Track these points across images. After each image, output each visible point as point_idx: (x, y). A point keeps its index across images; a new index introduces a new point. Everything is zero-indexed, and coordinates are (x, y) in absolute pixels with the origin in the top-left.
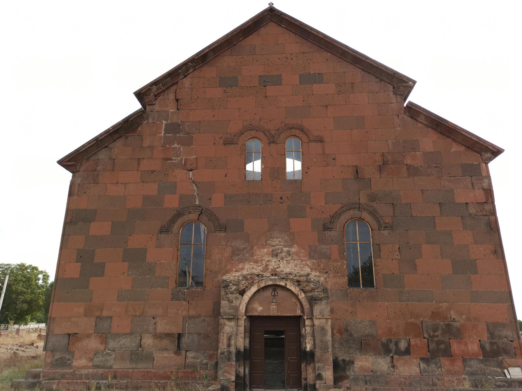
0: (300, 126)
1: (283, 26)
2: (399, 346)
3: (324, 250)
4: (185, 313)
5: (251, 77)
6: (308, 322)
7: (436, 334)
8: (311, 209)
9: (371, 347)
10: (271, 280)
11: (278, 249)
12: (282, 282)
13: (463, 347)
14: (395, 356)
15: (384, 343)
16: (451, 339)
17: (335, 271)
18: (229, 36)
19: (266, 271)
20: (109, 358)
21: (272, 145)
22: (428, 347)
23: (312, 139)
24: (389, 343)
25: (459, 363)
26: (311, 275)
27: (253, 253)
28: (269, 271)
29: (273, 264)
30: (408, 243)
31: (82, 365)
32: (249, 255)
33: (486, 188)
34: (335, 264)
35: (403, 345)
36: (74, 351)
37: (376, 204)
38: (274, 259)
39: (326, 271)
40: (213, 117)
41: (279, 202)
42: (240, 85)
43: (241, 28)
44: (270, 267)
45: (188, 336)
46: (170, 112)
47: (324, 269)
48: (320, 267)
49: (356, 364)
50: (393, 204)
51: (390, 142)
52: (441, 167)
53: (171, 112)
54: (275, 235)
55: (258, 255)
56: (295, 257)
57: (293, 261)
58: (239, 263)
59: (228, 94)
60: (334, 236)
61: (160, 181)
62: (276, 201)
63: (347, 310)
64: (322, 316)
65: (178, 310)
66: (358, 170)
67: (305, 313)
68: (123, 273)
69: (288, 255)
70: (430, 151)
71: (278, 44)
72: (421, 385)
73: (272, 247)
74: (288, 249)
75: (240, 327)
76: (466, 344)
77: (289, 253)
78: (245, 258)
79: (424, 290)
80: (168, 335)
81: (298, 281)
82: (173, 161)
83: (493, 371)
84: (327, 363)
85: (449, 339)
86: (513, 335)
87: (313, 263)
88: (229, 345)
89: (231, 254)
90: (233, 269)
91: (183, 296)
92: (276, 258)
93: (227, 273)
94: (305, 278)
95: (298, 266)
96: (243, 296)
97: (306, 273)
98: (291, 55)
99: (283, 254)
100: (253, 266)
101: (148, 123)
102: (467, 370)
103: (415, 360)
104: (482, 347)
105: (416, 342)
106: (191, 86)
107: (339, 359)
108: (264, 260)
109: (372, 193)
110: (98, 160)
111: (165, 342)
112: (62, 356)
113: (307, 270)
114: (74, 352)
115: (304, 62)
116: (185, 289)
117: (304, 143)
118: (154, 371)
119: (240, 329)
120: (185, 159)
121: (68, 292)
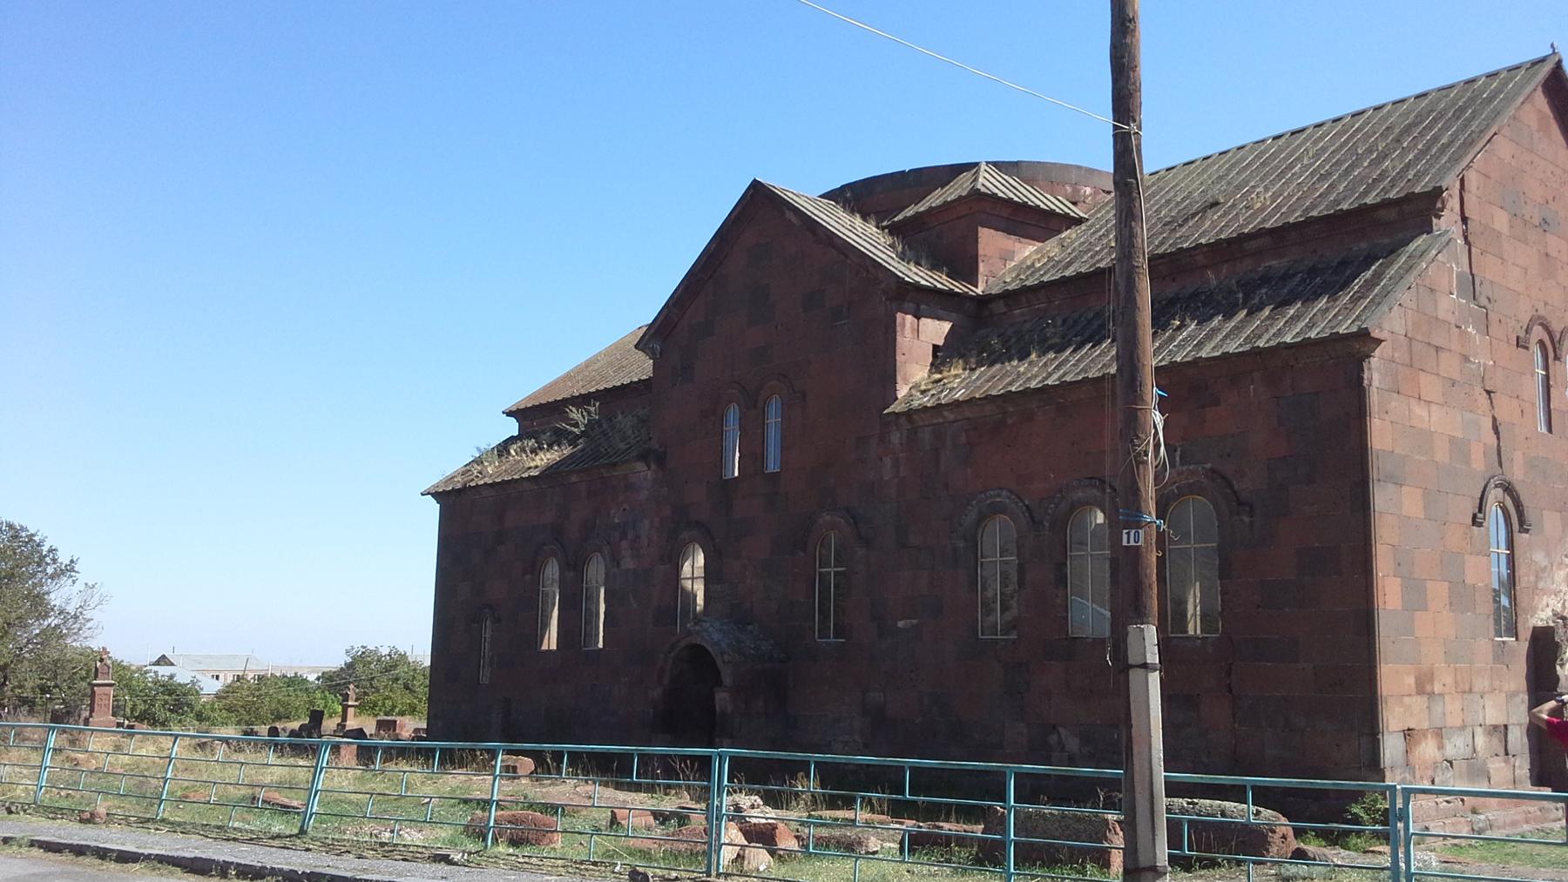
4: (1506, 688)
80: (1495, 727)
112: (1403, 776)
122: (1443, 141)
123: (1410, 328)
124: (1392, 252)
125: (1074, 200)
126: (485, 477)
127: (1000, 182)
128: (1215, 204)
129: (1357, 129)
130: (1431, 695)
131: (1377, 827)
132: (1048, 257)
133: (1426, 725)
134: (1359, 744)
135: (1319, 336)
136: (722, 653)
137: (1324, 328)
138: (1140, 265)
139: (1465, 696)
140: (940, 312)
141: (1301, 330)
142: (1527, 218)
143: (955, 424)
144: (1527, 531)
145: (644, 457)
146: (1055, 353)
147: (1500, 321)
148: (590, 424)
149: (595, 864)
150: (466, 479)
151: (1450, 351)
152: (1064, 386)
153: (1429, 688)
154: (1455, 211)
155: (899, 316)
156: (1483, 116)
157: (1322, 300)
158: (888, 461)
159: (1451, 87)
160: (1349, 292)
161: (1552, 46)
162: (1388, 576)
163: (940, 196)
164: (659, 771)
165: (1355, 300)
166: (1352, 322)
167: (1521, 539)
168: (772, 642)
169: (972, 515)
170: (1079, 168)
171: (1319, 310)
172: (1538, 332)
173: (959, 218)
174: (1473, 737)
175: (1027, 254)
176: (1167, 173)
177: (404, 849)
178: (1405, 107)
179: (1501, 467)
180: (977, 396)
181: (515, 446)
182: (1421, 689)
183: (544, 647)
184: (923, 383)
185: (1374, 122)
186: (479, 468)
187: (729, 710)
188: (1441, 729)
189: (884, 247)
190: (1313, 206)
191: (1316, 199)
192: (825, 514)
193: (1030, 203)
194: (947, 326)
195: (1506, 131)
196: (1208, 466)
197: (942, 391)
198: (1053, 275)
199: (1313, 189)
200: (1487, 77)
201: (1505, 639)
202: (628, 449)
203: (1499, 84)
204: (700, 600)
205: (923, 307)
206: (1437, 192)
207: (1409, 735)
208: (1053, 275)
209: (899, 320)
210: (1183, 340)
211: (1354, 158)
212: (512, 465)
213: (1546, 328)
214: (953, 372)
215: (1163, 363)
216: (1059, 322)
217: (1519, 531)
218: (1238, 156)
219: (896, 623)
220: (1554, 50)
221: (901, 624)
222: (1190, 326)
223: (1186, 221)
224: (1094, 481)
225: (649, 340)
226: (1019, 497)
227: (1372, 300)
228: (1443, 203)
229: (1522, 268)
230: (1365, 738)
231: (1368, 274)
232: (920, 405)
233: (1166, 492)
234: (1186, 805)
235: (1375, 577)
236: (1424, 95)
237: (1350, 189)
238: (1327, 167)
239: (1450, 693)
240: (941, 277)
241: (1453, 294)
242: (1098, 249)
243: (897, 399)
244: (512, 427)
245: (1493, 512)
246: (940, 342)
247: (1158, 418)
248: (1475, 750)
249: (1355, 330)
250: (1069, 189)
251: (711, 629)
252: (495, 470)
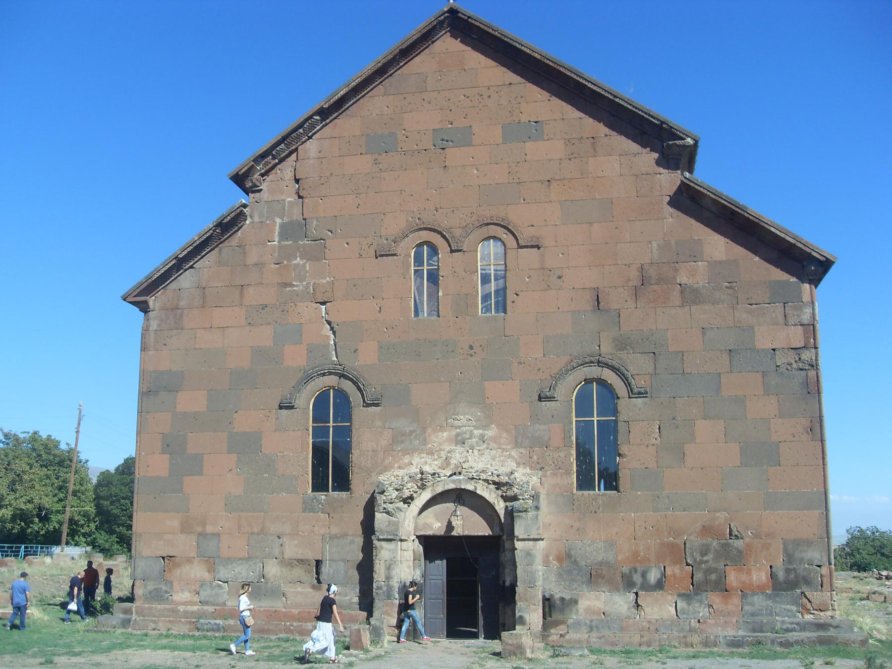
0: (503, 220)
1: (473, 36)
2: (648, 577)
3: (539, 432)
5: (419, 133)
7: (705, 559)
8: (520, 365)
9: (605, 580)
10: (454, 482)
11: (465, 433)
12: (469, 485)
13: (744, 577)
14: (640, 593)
15: (625, 573)
16: (728, 565)
17: (556, 465)
18: (379, 62)
19: (447, 467)
20: (220, 591)
22: (692, 578)
23: (522, 243)
24: (633, 573)
25: (736, 600)
26: (516, 473)
27: (425, 440)
28: (452, 467)
29: (458, 455)
30: (674, 419)
31: (186, 600)
32: (420, 442)
33: (806, 322)
34: (556, 455)
35: (653, 576)
36: (172, 580)
37: (626, 355)
38: (459, 449)
39: (541, 466)
40: (358, 207)
41: (468, 355)
42: (401, 148)
43: (401, 48)
44: (453, 462)
45: (330, 563)
46: (287, 203)
47: (538, 463)
48: (531, 460)
49: (581, 605)
51: (654, 244)
52: (736, 289)
53: (290, 202)
54: (461, 409)
55: (434, 442)
56: (492, 445)
57: (489, 450)
58: (404, 455)
59: (381, 166)
60: (555, 410)
61: (276, 322)
62: (462, 353)
63: (572, 527)
64: (528, 535)
65: (314, 526)
66: (599, 295)
67: (505, 531)
68: (230, 470)
69: (481, 441)
70: (720, 260)
71: (465, 71)
72: (672, 630)
73: (456, 429)
74: (481, 431)
75: (405, 552)
76: (749, 572)
77: (482, 439)
78: (413, 447)
79: (694, 493)
80: (301, 561)
81: (494, 483)
82: (294, 288)
83: (785, 609)
84: (533, 602)
85: (725, 566)
86: (821, 557)
87: (521, 453)
88: (388, 578)
89: (391, 442)
90: (394, 464)
91: (320, 506)
92: (462, 447)
94: (507, 478)
95: (498, 458)
96: (409, 506)
97: (509, 470)
98: (489, 89)
99: (473, 440)
100: (426, 459)
101: (252, 224)
102: (746, 609)
103: (670, 597)
104: (773, 576)
105: (673, 571)
106: (319, 154)
107: (556, 597)
108: (444, 450)
109: (621, 336)
110: (180, 290)
111: (298, 572)
112: (156, 587)
113: (511, 465)
115: (510, 101)
116: (323, 495)
117: (509, 250)
118: (284, 610)
119: (405, 555)
120: (314, 284)
121: (155, 498)
130: (202, 535)
133: (193, 554)
144: (377, 405)
147: (347, 244)
182: (186, 528)
217: (363, 406)
241: (274, 241)
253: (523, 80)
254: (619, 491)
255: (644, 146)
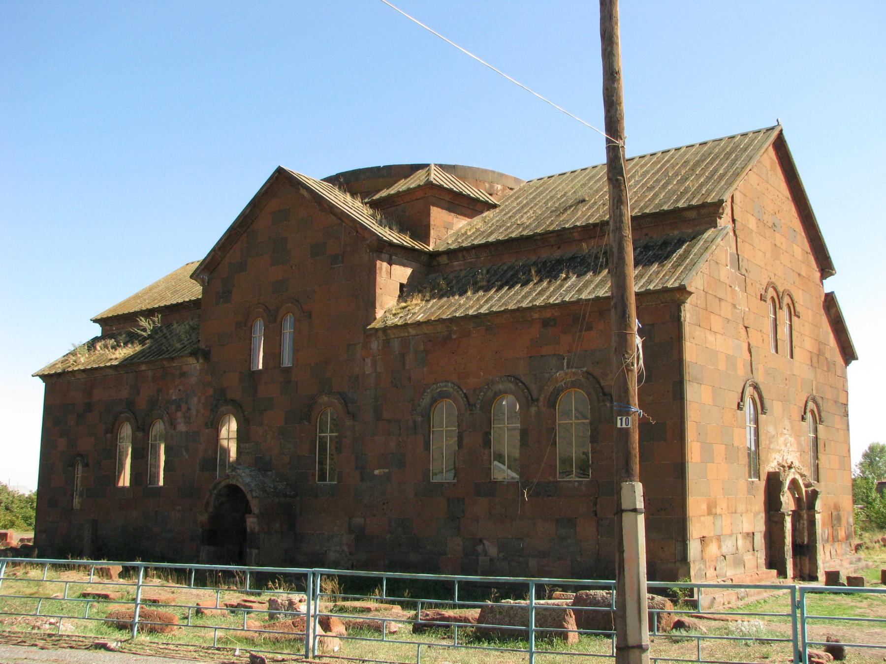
6: (805, 517)
10: (794, 473)
21: (781, 310)
25: (840, 546)
28: (784, 462)
39: (803, 464)
44: (785, 458)
50: (822, 398)
56: (793, 448)
80: (748, 534)
93: (769, 464)
114: (706, 561)
122: (720, 172)
123: (706, 286)
124: (694, 238)
125: (490, 193)
126: (78, 364)
127: (444, 178)
128: (583, 201)
129: (666, 161)
131: (686, 598)
132: (476, 228)
133: (712, 534)
134: (675, 547)
135: (655, 288)
136: (251, 491)
137: (658, 283)
138: (627, 235)
139: (733, 515)
140: (405, 261)
141: (643, 284)
142: (765, 222)
143: (416, 337)
144: (765, 413)
145: (194, 354)
146: (484, 291)
148: (155, 331)
149: (218, 649)
150: (64, 366)
151: (726, 301)
152: (491, 314)
153: (714, 511)
154: (729, 215)
155: (378, 263)
156: (742, 159)
157: (655, 265)
158: (369, 361)
159: (721, 140)
160: (671, 262)
161: (777, 120)
162: (694, 441)
163: (405, 184)
164: (220, 574)
165: (676, 267)
166: (675, 280)
167: (762, 418)
168: (285, 483)
169: (426, 400)
170: (493, 172)
171: (653, 272)
172: (771, 292)
173: (417, 199)
174: (737, 541)
175: (461, 226)
176: (549, 179)
177: (67, 638)
178: (694, 150)
179: (752, 373)
180: (433, 319)
181: (100, 344)
182: (710, 512)
183: (121, 484)
184: (394, 309)
185: (676, 157)
186: (74, 358)
187: (257, 530)
188: (720, 536)
189: (367, 216)
190: (646, 207)
191: (646, 202)
192: (324, 396)
193: (464, 193)
194: (409, 271)
195: (755, 170)
196: (585, 369)
197: (408, 314)
198: (480, 240)
199: (644, 196)
200: (741, 135)
201: (753, 479)
202: (183, 348)
203: (749, 140)
204: (233, 454)
205: (394, 257)
206: (721, 202)
207: (703, 541)
208: (480, 240)
209: (378, 265)
210: (568, 287)
211: (667, 178)
212: (98, 357)
213: (775, 289)
214: (414, 302)
215: (557, 302)
216: (485, 272)
217: (762, 414)
218: (594, 172)
219: (373, 472)
220: (778, 123)
221: (376, 472)
222: (572, 278)
223: (566, 210)
224: (510, 378)
225: (200, 272)
226: (459, 387)
227: (686, 267)
228: (723, 209)
229: (763, 253)
230: (679, 542)
231: (681, 251)
232: (392, 323)
233: (557, 386)
234: (605, 594)
235: (686, 442)
236: (705, 143)
237: (668, 198)
238: (651, 183)
239: (725, 514)
240: (405, 238)
242: (509, 225)
243: (375, 319)
244: (97, 330)
245: (748, 401)
246: (405, 282)
247: (638, 341)
248: (737, 548)
249: (677, 286)
250: (487, 185)
251: (243, 474)
252: (86, 360)
253: (791, 199)
254: (818, 482)
255: (818, 267)
